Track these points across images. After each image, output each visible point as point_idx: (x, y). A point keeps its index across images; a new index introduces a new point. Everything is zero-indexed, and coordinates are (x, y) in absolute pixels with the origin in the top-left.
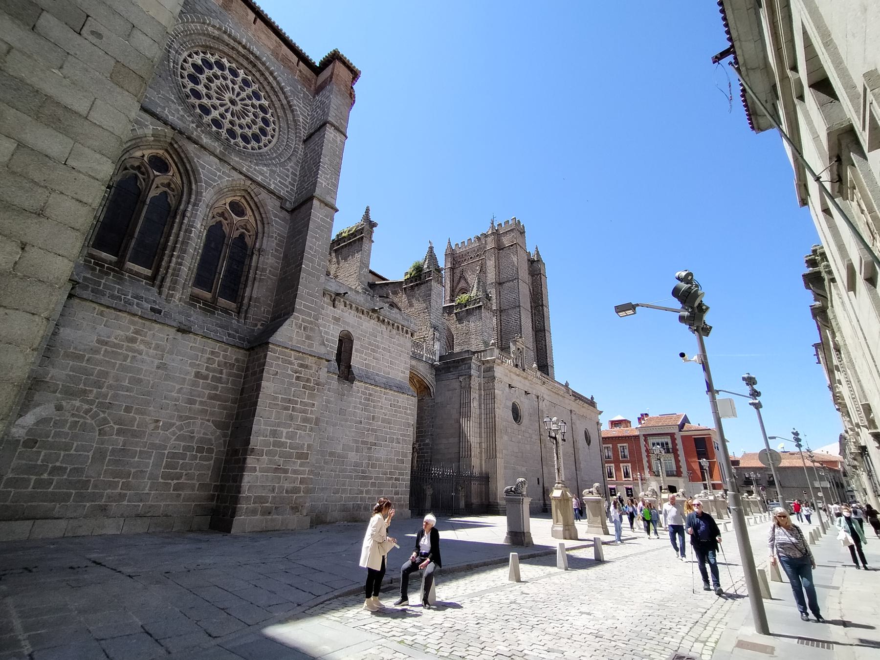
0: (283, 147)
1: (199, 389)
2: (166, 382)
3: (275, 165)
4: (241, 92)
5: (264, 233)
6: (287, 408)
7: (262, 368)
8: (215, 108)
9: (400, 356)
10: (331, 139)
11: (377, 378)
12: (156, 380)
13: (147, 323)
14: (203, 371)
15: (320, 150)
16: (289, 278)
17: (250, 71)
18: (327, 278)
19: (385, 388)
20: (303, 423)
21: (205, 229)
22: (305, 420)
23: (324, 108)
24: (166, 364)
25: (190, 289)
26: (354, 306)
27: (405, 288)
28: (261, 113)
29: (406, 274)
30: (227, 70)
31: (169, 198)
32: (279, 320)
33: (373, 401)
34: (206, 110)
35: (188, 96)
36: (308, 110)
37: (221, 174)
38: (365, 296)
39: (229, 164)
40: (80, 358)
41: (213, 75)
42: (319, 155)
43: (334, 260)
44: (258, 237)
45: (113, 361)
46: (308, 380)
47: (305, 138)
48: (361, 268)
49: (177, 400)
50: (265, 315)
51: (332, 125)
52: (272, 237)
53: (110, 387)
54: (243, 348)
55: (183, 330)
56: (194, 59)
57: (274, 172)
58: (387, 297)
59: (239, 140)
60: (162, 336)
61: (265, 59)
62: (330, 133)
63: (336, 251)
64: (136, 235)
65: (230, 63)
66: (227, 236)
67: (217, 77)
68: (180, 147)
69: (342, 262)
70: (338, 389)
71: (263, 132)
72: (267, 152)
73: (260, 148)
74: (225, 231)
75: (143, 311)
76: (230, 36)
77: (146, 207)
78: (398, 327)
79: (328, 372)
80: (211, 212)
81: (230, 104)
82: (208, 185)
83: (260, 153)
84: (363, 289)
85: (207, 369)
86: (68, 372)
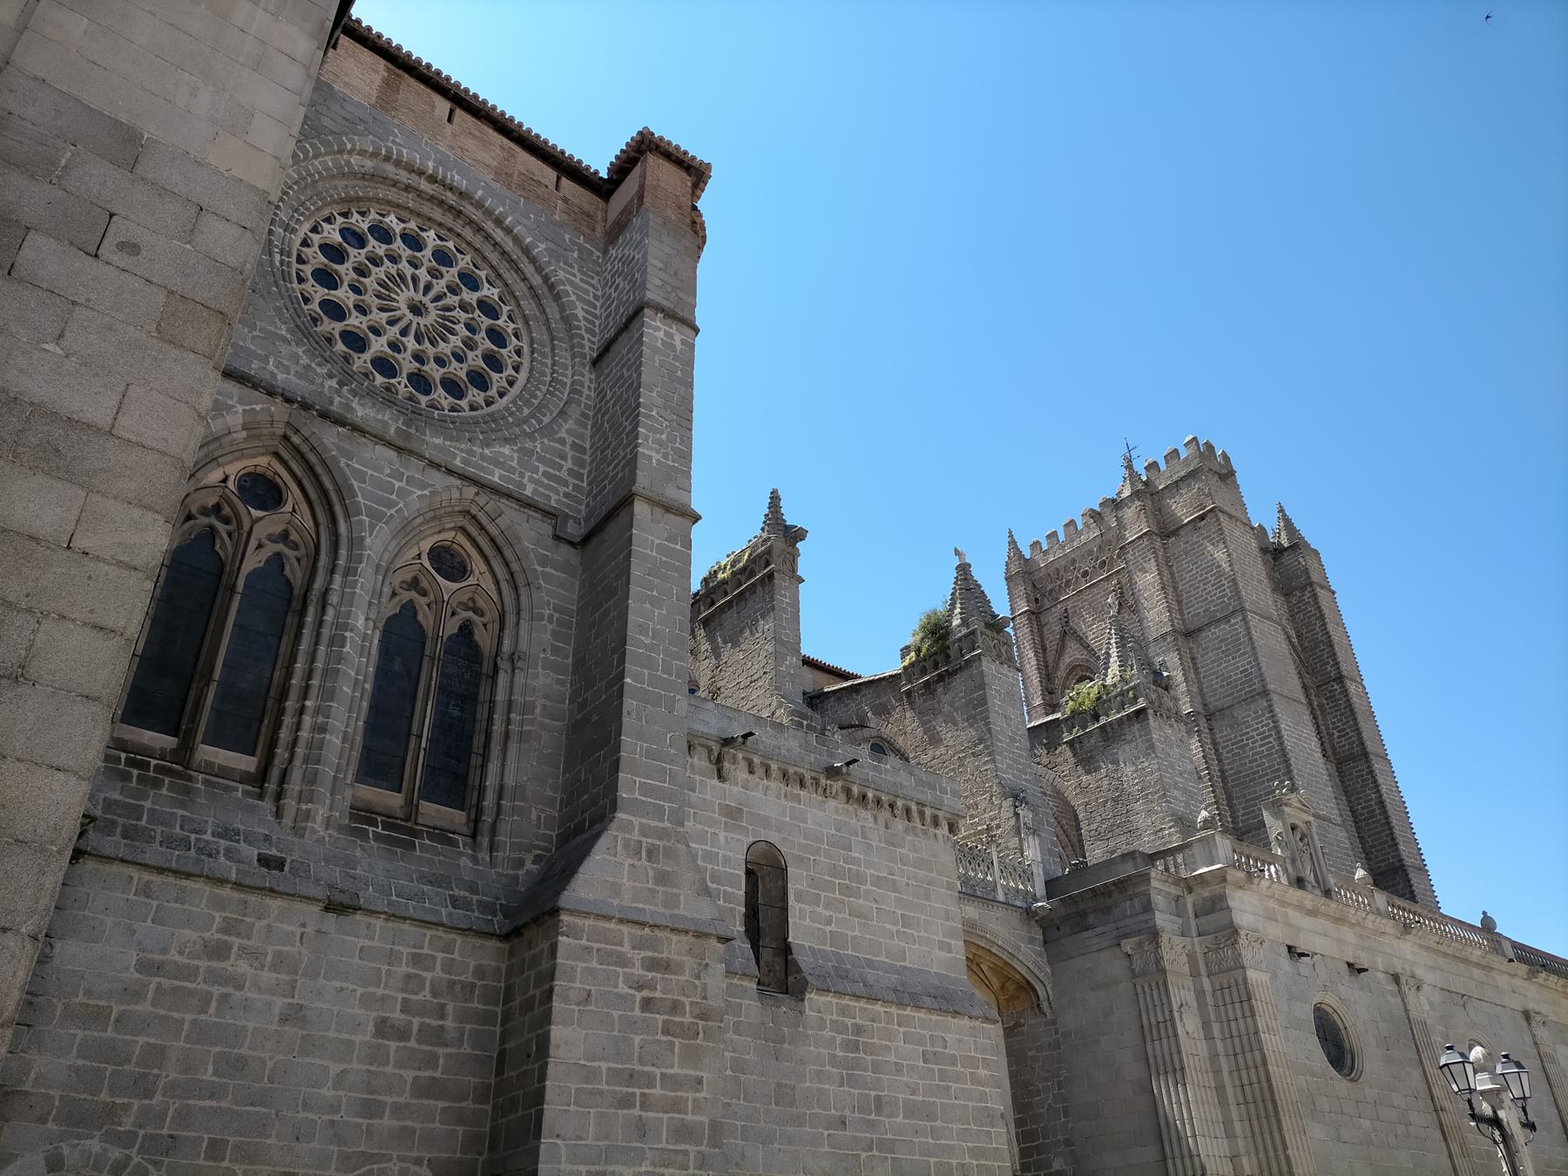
0: (544, 389)
1: (389, 1069)
2: (307, 1060)
3: (531, 436)
4: (434, 281)
5: (519, 610)
6: (625, 1102)
7: (547, 987)
8: (377, 331)
9: (927, 897)
10: (659, 344)
11: (871, 975)
12: (281, 1057)
13: (253, 898)
14: (397, 1016)
15: (635, 375)
16: (595, 718)
17: (450, 230)
18: (693, 701)
19: (901, 1004)
20: (676, 1143)
21: (375, 627)
22: (683, 1132)
23: (633, 273)
24: (301, 1006)
26: (774, 766)
27: (908, 693)
28: (484, 318)
29: (905, 651)
30: (399, 239)
31: (287, 568)
32: (579, 839)
33: (869, 1049)
34: (356, 342)
35: (315, 320)
36: (593, 286)
37: (403, 484)
38: (800, 734)
39: (421, 457)
40: (96, 1016)
41: (367, 259)
42: (635, 388)
43: (703, 648)
44: (507, 625)
45: (176, 1015)
46: (675, 1007)
47: (595, 355)
48: (778, 657)
49: (334, 1108)
50: (541, 831)
51: (659, 308)
52: (541, 617)
53: (172, 1089)
54: (492, 935)
55: (338, 907)
56: (325, 234)
57: (530, 453)
58: (862, 726)
59: (439, 393)
60: (289, 928)
61: (480, 193)
62: (655, 329)
63: (706, 622)
64: (217, 675)
65: (403, 221)
66: (430, 635)
67: (376, 261)
68: (306, 440)
69: (727, 652)
70: (763, 1024)
71: (494, 362)
72: (507, 409)
73: (488, 404)
74: (424, 623)
75: (242, 866)
76: (398, 163)
78: (908, 811)
79: (730, 973)
80: (387, 583)
81: (410, 316)
82: (376, 516)
83: (491, 415)
84: (793, 713)
85: (406, 1007)
86: (72, 1059)
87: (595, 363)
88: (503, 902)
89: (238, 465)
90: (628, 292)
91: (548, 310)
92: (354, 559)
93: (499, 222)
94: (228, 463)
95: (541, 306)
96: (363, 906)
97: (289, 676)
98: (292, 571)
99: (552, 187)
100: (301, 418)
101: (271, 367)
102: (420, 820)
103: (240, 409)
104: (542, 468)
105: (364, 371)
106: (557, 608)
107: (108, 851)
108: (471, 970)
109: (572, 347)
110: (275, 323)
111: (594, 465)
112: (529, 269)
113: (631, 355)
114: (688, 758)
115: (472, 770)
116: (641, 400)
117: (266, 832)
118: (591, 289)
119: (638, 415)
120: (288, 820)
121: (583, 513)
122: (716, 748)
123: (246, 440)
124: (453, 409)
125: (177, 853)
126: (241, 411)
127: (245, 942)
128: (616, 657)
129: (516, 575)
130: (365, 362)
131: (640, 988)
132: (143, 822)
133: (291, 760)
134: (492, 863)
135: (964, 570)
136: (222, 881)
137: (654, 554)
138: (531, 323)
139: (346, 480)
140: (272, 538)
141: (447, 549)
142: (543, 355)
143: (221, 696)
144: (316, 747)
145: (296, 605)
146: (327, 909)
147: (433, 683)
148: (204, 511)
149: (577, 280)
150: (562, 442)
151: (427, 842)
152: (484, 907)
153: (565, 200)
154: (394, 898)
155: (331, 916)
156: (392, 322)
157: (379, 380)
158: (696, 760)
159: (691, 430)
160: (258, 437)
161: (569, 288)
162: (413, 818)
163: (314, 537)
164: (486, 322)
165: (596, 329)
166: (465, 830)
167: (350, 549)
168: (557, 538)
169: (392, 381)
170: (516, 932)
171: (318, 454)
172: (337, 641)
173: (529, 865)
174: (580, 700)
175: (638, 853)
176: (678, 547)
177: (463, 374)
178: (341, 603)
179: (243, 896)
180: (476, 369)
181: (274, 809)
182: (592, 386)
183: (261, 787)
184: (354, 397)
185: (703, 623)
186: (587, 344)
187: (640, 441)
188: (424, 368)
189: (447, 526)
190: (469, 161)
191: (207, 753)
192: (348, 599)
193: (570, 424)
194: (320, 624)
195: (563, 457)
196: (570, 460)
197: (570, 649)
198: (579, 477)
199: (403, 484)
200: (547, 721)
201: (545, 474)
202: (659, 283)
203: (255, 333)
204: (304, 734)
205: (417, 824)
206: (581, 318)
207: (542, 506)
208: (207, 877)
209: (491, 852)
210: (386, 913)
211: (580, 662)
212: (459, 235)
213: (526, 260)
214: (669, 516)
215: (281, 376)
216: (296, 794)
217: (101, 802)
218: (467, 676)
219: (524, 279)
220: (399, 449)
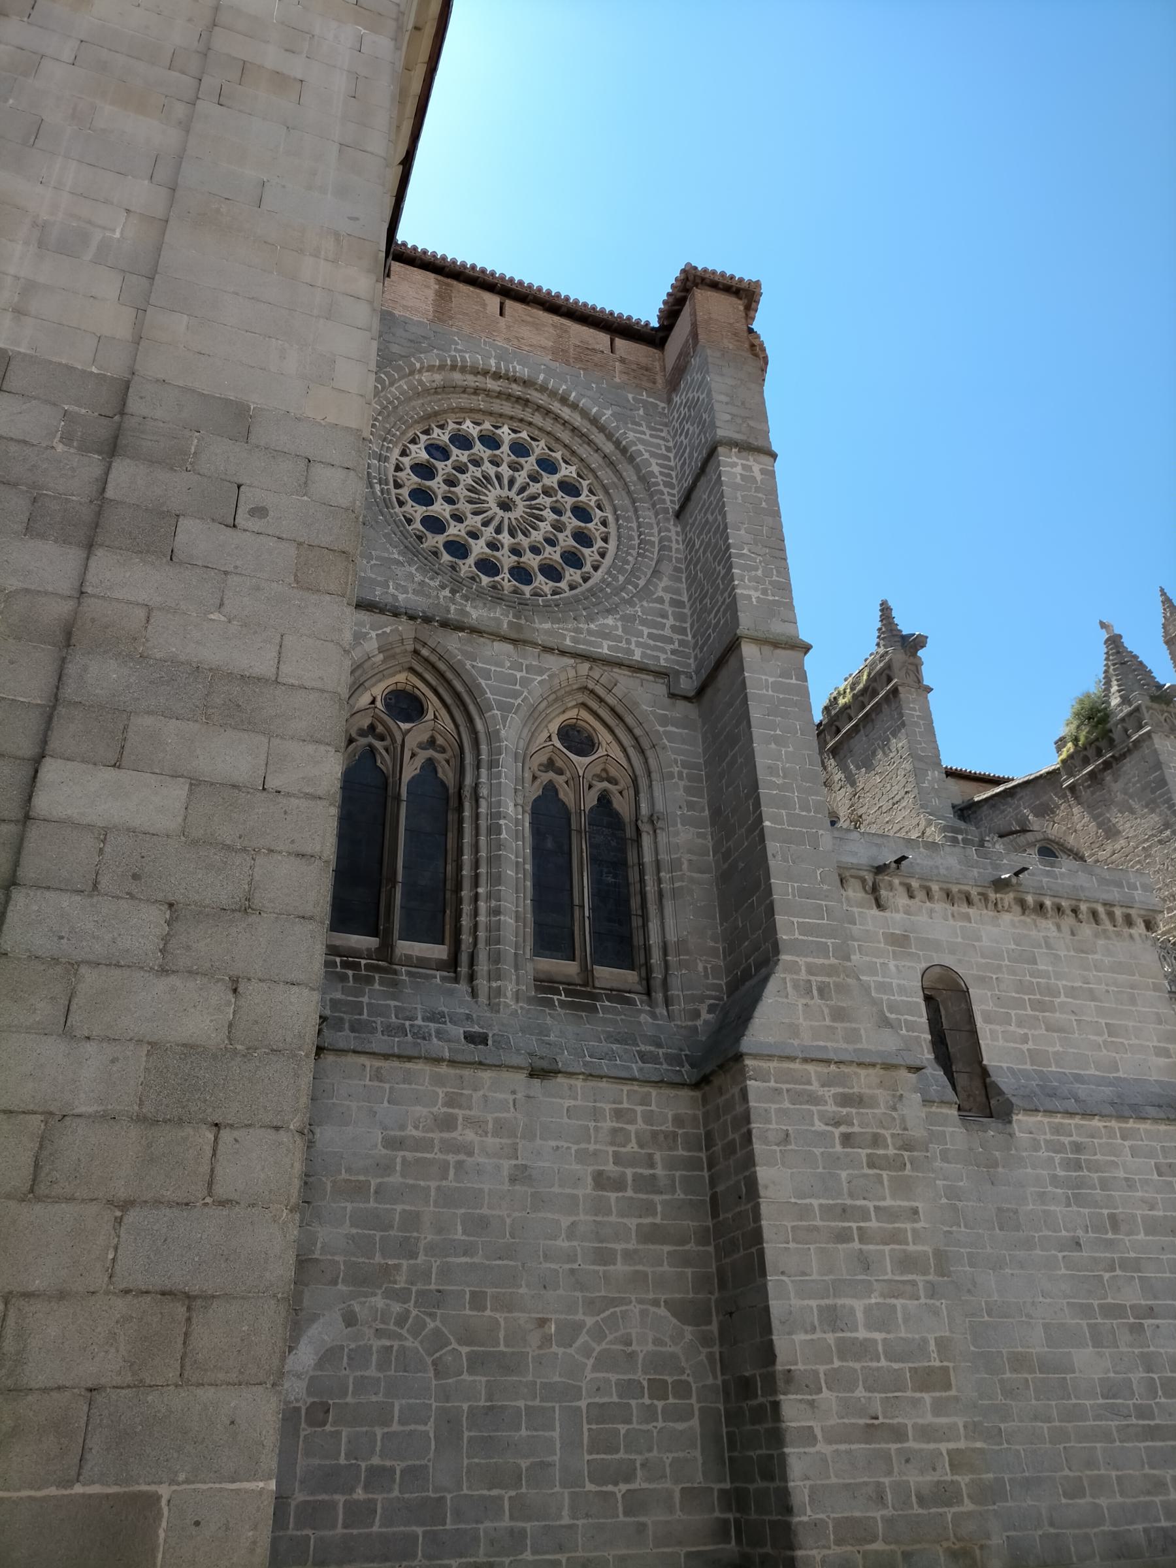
0: (634, 553)
1: (613, 1219)
2: (541, 1215)
3: (630, 602)
4: (516, 474)
5: (649, 774)
6: (843, 1237)
7: (744, 1130)
8: (474, 535)
9: (1133, 1001)
10: (738, 480)
11: (1082, 1090)
12: (517, 1214)
13: (467, 1073)
14: (610, 1168)
15: (719, 518)
16: (741, 865)
17: (521, 420)
18: (836, 834)
19: (1121, 1117)
20: (902, 1273)
21: (524, 812)
22: (907, 1263)
23: (701, 414)
24: (525, 1167)
25: (530, 966)
26: (935, 887)
27: (1072, 788)
28: (567, 498)
29: (1060, 743)
30: (478, 442)
31: (440, 770)
32: (748, 984)
33: (1094, 1167)
34: (458, 549)
35: (420, 538)
36: (663, 438)
37: (524, 674)
38: (957, 850)
39: (534, 644)
40: (358, 1190)
41: (453, 468)
42: (722, 531)
43: (836, 778)
45: (422, 1183)
46: (876, 1141)
47: (677, 507)
48: (918, 774)
49: (572, 1258)
50: (710, 981)
51: (732, 444)
52: (671, 776)
53: (431, 1249)
54: (682, 1085)
55: (541, 1072)
56: (414, 455)
58: (1024, 831)
61: (542, 377)
62: (732, 466)
63: (834, 751)
64: (400, 878)
65: (478, 424)
66: (573, 811)
67: (461, 469)
68: (433, 650)
69: (862, 777)
70: (971, 1149)
71: (583, 538)
72: (603, 580)
73: (586, 579)
75: (453, 1045)
76: (463, 370)
77: (404, 806)
78: (1094, 914)
79: (927, 1102)
80: (527, 768)
81: (501, 513)
82: (506, 708)
83: (590, 590)
84: (944, 829)
85: (618, 1159)
86: (347, 1229)
87: (678, 515)
88: (688, 1053)
89: (383, 685)
90: (699, 434)
91: (624, 474)
92: (495, 752)
93: (564, 400)
94: (373, 685)
95: (617, 472)
96: (563, 1070)
97: (459, 867)
98: (444, 772)
99: (607, 351)
100: (425, 631)
101: (391, 590)
102: (597, 984)
103: (373, 634)
104: (646, 631)
105: (470, 575)
106: (685, 765)
107: (342, 1045)
108: (670, 1119)
109: (654, 505)
110: (388, 549)
111: (695, 617)
112: (599, 438)
113: (712, 498)
114: (842, 892)
115: (635, 932)
116: (730, 541)
117: (467, 1012)
118: (661, 442)
119: (730, 557)
120: (483, 999)
121: (693, 666)
122: (869, 878)
123: (384, 661)
124: (554, 593)
125: (397, 1039)
126: (374, 636)
127: (467, 1112)
128: (751, 802)
129: (641, 740)
130: (470, 567)
131: (837, 1124)
132: (365, 1016)
133: (475, 943)
134: (670, 1017)
135: (1114, 643)
136: (438, 1060)
137: (770, 693)
138: (611, 491)
139: (474, 680)
140: (422, 746)
141: (573, 727)
142: (628, 519)
143: (406, 895)
144: (495, 929)
145: (453, 803)
147: (584, 854)
148: (362, 733)
149: (647, 437)
150: (661, 600)
151: (607, 1003)
152: (670, 1059)
153: (623, 361)
154: (588, 1059)
155: (536, 1082)
156: (486, 524)
157: (485, 580)
158: (850, 893)
159: (785, 559)
160: (393, 656)
161: (641, 447)
162: (591, 983)
163: (456, 737)
164: (569, 501)
165: (674, 481)
166: (639, 988)
167: (490, 743)
168: (672, 696)
169: (497, 578)
171: (447, 662)
172: (494, 829)
173: (705, 1016)
174: (724, 850)
175: (809, 992)
176: (794, 681)
177: (557, 557)
178: (490, 795)
179: (458, 1071)
180: (569, 549)
181: (470, 990)
182: (680, 539)
183: (455, 972)
184: (467, 601)
185: (832, 752)
186: (667, 498)
187: (736, 583)
188: (522, 560)
189: (570, 705)
190: (526, 348)
191: (406, 948)
192: (496, 789)
193: (665, 582)
194: (477, 816)
195: (664, 615)
196: (671, 617)
197: (704, 801)
198: (683, 631)
199: (524, 674)
200: (695, 875)
201: (650, 636)
202: (728, 417)
203: (372, 563)
204: (482, 918)
205: (594, 987)
206: (657, 474)
207: (652, 668)
208: (426, 1058)
209: (667, 1007)
210: (583, 1073)
211: (716, 812)
212: (530, 424)
213: (594, 430)
214: (779, 652)
215: (401, 597)
216: (485, 973)
217: (328, 1002)
218: (614, 844)
219: (597, 450)
220: (514, 641)
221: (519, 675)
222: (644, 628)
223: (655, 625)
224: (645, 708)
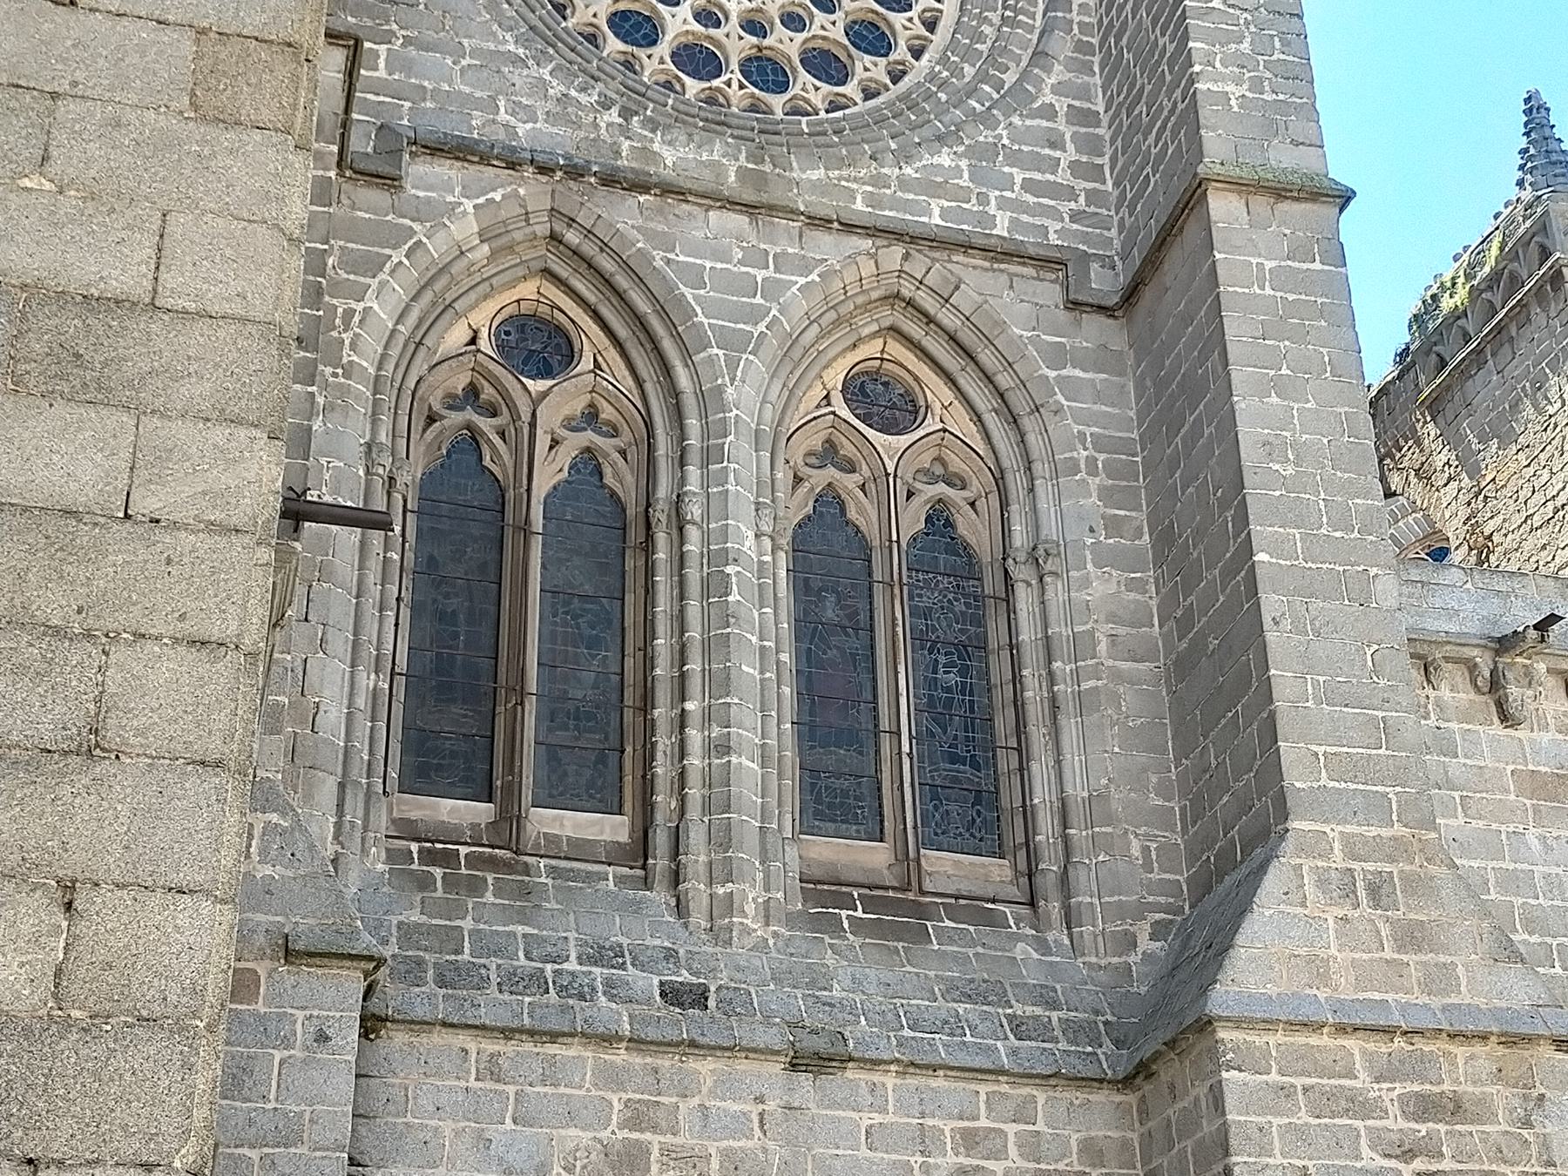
0: (995, 17)
3: (987, 120)
13: (665, 1062)
25: (792, 852)
37: (770, 272)
39: (792, 213)
44: (1013, 495)
57: (993, 149)
59: (804, 82)
60: (736, 1107)
66: (876, 543)
72: (932, 77)
73: (896, 78)
74: (861, 522)
80: (780, 462)
82: (735, 344)
88: (1109, 1017)
89: (491, 306)
92: (715, 431)
94: (472, 308)
96: (856, 1055)
97: (649, 662)
98: (616, 474)
100: (572, 196)
101: (503, 116)
102: (928, 886)
103: (469, 205)
105: (662, 78)
106: (1099, 444)
107: (420, 1012)
108: (1075, 1150)
110: (494, 34)
111: (1119, 142)
114: (1429, 691)
115: (1003, 780)
117: (666, 944)
119: (1184, 17)
122: (1484, 662)
123: (493, 256)
124: (833, 107)
125: (527, 999)
126: (471, 210)
127: (669, 1139)
128: (1230, 514)
129: (1010, 396)
130: (662, 61)
131: (1408, 1155)
132: (466, 956)
134: (1075, 949)
136: (609, 1039)
139: (672, 289)
140: (571, 425)
141: (874, 375)
143: (551, 717)
145: (635, 535)
146: (794, 1066)
147: (900, 630)
148: (453, 403)
151: (948, 923)
152: (1074, 1031)
154: (907, 1033)
155: (805, 1080)
157: (693, 86)
158: (1445, 693)
160: (510, 248)
162: (915, 884)
163: (640, 406)
166: (1013, 892)
167: (704, 415)
168: (1074, 305)
170: (1142, 1071)
171: (616, 255)
172: (716, 585)
173: (1145, 944)
174: (1179, 613)
175: (1349, 892)
177: (838, 33)
178: (707, 515)
179: (649, 1060)
180: (861, 16)
181: (673, 902)
183: (644, 867)
184: (653, 131)
185: (1429, 408)
188: (766, 42)
189: (866, 331)
191: (546, 821)
192: (718, 505)
193: (1058, 74)
195: (1056, 143)
196: (1070, 147)
197: (1141, 517)
198: (1096, 173)
199: (770, 272)
200: (1125, 665)
201: (1028, 185)
203: (464, 62)
205: (922, 893)
207: (1032, 251)
208: (583, 1034)
209: (1069, 928)
210: (897, 1061)
211: (1164, 538)
215: (522, 129)
217: (394, 931)
218: (959, 607)
220: (749, 208)
221: (760, 275)
222: (1015, 170)
223: (1038, 163)
224: (1018, 331)
